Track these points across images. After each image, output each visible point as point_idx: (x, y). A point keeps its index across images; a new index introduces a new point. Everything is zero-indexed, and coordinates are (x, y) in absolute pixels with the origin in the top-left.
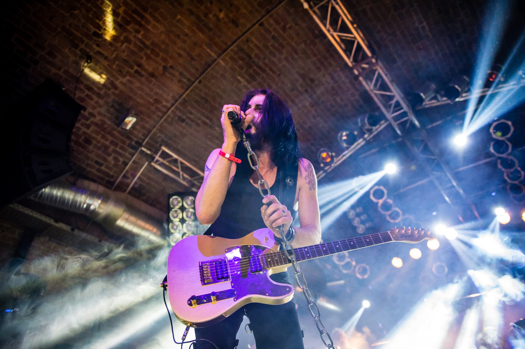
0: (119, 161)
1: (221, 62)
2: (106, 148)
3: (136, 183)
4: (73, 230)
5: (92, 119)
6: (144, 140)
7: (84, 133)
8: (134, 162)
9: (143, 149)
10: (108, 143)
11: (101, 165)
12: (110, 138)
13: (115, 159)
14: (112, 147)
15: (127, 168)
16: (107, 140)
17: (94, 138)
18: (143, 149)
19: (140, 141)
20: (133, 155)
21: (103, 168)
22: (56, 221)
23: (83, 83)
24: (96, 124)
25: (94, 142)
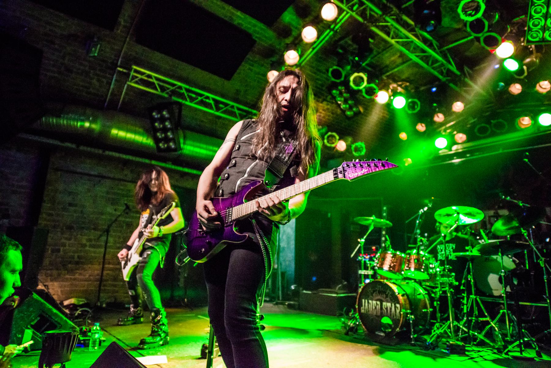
0: (103, 82)
3: (124, 98)
4: (78, 146)
8: (116, 80)
9: (119, 69)
10: (87, 68)
13: (98, 80)
15: (112, 87)
18: (119, 69)
19: (115, 62)
25: (75, 70)
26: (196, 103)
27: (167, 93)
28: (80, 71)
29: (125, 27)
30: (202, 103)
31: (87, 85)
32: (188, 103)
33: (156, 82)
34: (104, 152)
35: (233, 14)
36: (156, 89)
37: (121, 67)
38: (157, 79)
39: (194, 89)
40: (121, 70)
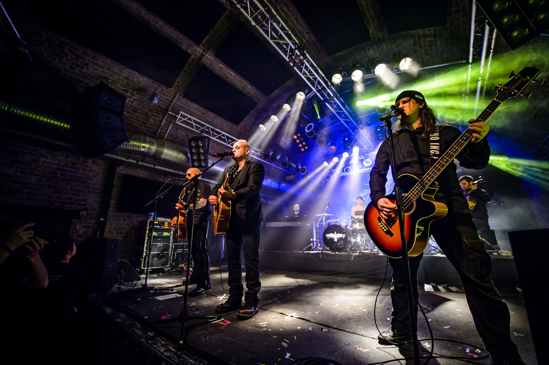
0: (157, 120)
1: (207, 55)
2: (147, 114)
5: (134, 97)
6: (169, 107)
7: (131, 106)
9: (169, 112)
10: (147, 111)
11: (147, 123)
12: (148, 108)
13: (154, 120)
14: (151, 113)
16: (146, 109)
17: (138, 109)
18: (169, 112)
20: (164, 116)
21: (148, 125)
22: (127, 159)
23: (122, 76)
24: (137, 100)
26: (216, 138)
27: (199, 131)
28: (142, 112)
29: (178, 86)
30: (220, 138)
31: (146, 121)
32: (212, 138)
33: (193, 123)
34: (155, 166)
35: (246, 86)
36: (194, 128)
37: (170, 111)
38: (195, 122)
39: (216, 129)
40: (171, 113)
